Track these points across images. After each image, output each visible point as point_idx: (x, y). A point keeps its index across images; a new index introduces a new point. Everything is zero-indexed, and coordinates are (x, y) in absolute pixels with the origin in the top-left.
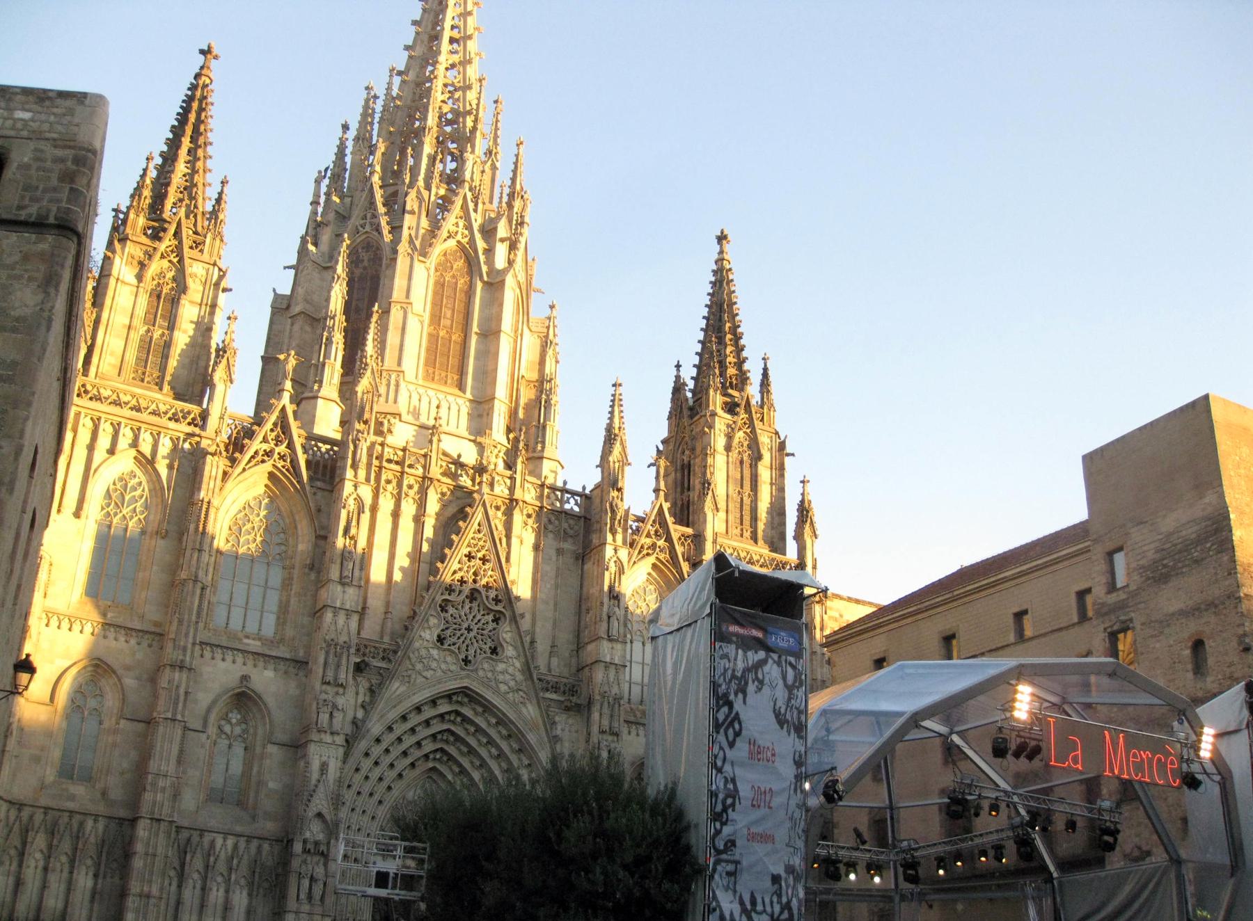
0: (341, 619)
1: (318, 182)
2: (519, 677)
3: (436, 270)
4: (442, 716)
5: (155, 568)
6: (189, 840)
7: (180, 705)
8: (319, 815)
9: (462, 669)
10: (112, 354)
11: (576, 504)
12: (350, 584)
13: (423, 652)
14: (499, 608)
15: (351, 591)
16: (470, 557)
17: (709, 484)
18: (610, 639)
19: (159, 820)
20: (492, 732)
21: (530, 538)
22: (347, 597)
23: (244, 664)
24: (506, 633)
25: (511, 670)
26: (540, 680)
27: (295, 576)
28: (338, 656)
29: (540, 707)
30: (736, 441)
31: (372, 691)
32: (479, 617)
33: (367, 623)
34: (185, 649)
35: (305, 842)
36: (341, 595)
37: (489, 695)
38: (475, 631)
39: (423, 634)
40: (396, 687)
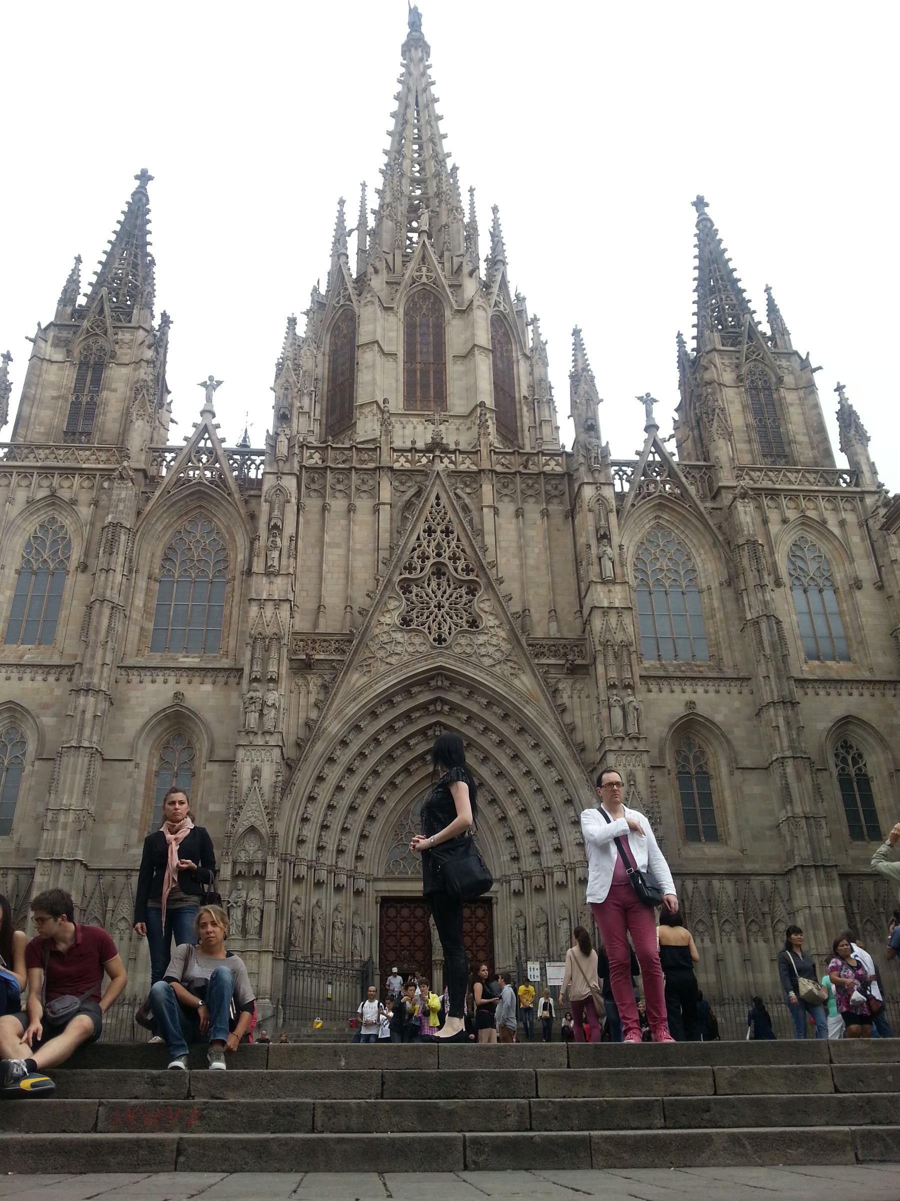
0: (269, 610)
2: (505, 647)
3: (406, 314)
4: (424, 707)
5: (75, 602)
6: (112, 885)
7: (87, 732)
8: (252, 829)
9: (436, 648)
10: (40, 424)
12: (277, 574)
13: (385, 638)
14: (472, 577)
15: (279, 581)
16: (430, 531)
17: (714, 410)
18: (604, 582)
19: (60, 861)
20: (486, 715)
21: (507, 508)
22: (274, 587)
23: (178, 683)
24: (483, 604)
25: (494, 641)
26: (529, 645)
27: (236, 587)
28: (267, 650)
29: (535, 676)
30: (744, 370)
31: (325, 687)
32: (448, 592)
33: (322, 621)
34: (91, 672)
35: (235, 863)
36: (267, 585)
37: (470, 672)
38: (447, 605)
39: (382, 619)
40: (356, 679)
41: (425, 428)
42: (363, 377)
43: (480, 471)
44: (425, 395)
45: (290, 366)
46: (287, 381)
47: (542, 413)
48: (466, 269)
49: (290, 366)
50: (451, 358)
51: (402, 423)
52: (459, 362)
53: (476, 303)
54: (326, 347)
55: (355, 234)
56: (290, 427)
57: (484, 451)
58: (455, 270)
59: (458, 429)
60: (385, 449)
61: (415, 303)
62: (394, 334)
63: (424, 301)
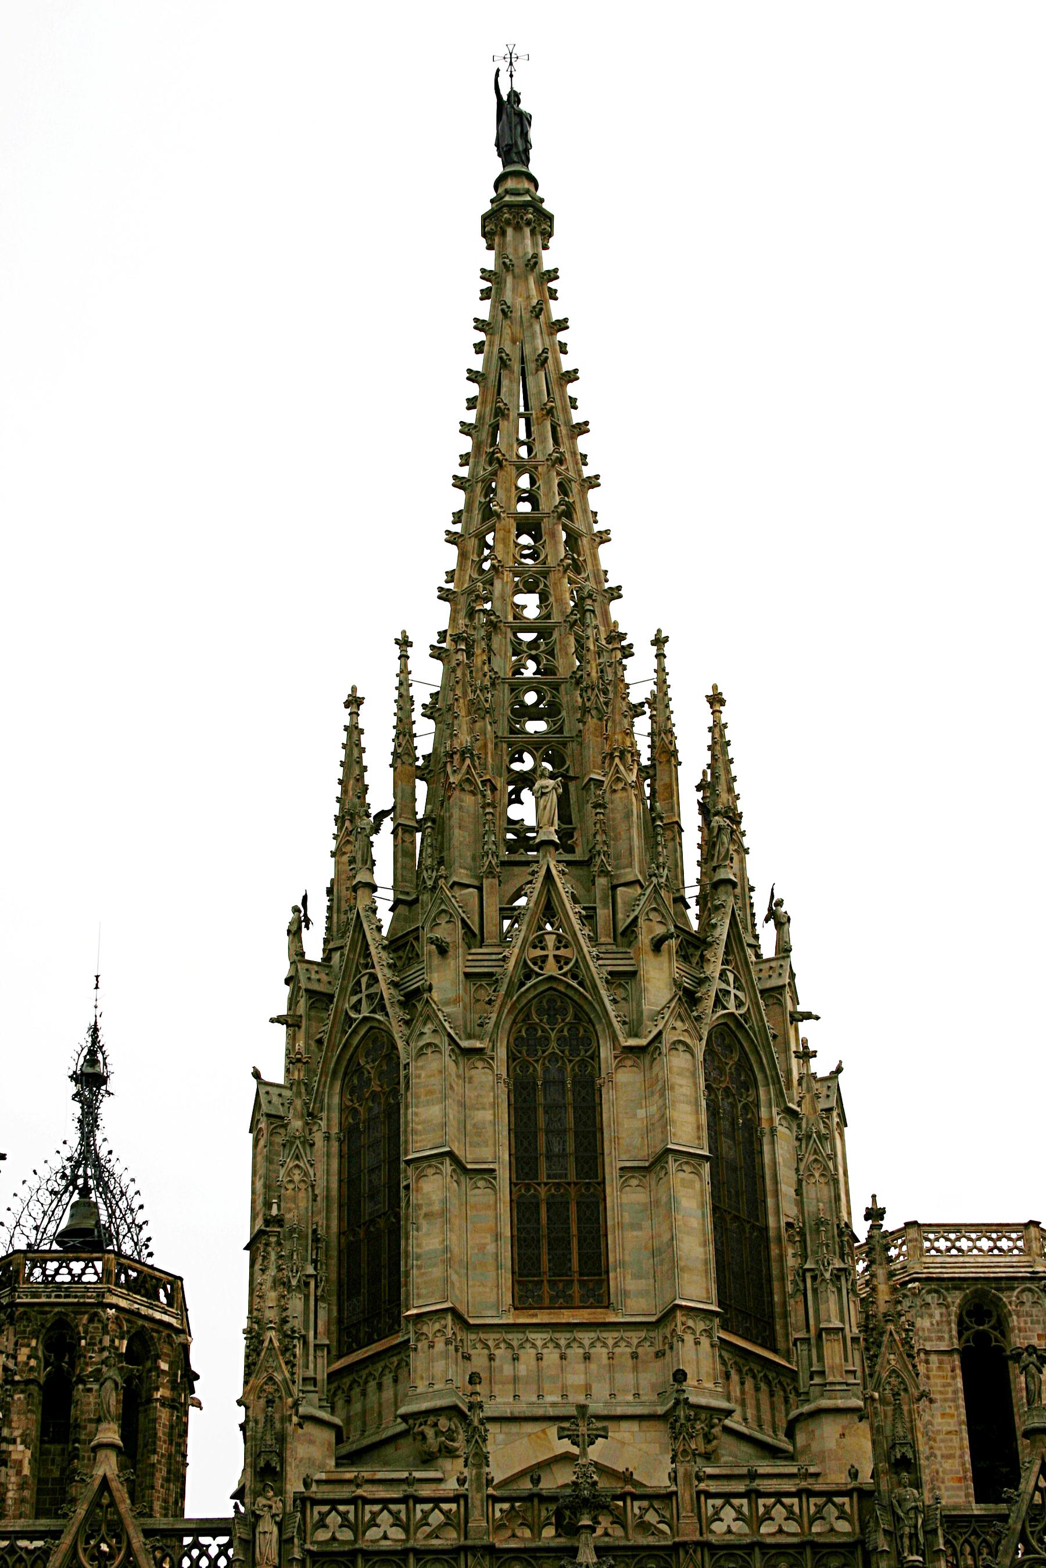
1: (294, 934)
3: (511, 1057)
11: (842, 1516)
41: (563, 1357)
42: (425, 1241)
43: (676, 1546)
44: (560, 1264)
45: (276, 1344)
46: (271, 1378)
47: (822, 1307)
48: (644, 939)
49: (276, 1344)
50: (616, 1173)
51: (510, 1346)
52: (634, 1182)
53: (669, 1037)
54: (330, 1121)
55: (388, 825)
56: (280, 1492)
57: (685, 1496)
58: (621, 928)
59: (635, 1356)
60: (476, 1499)
61: (532, 1028)
62: (487, 1115)
63: (552, 1022)
